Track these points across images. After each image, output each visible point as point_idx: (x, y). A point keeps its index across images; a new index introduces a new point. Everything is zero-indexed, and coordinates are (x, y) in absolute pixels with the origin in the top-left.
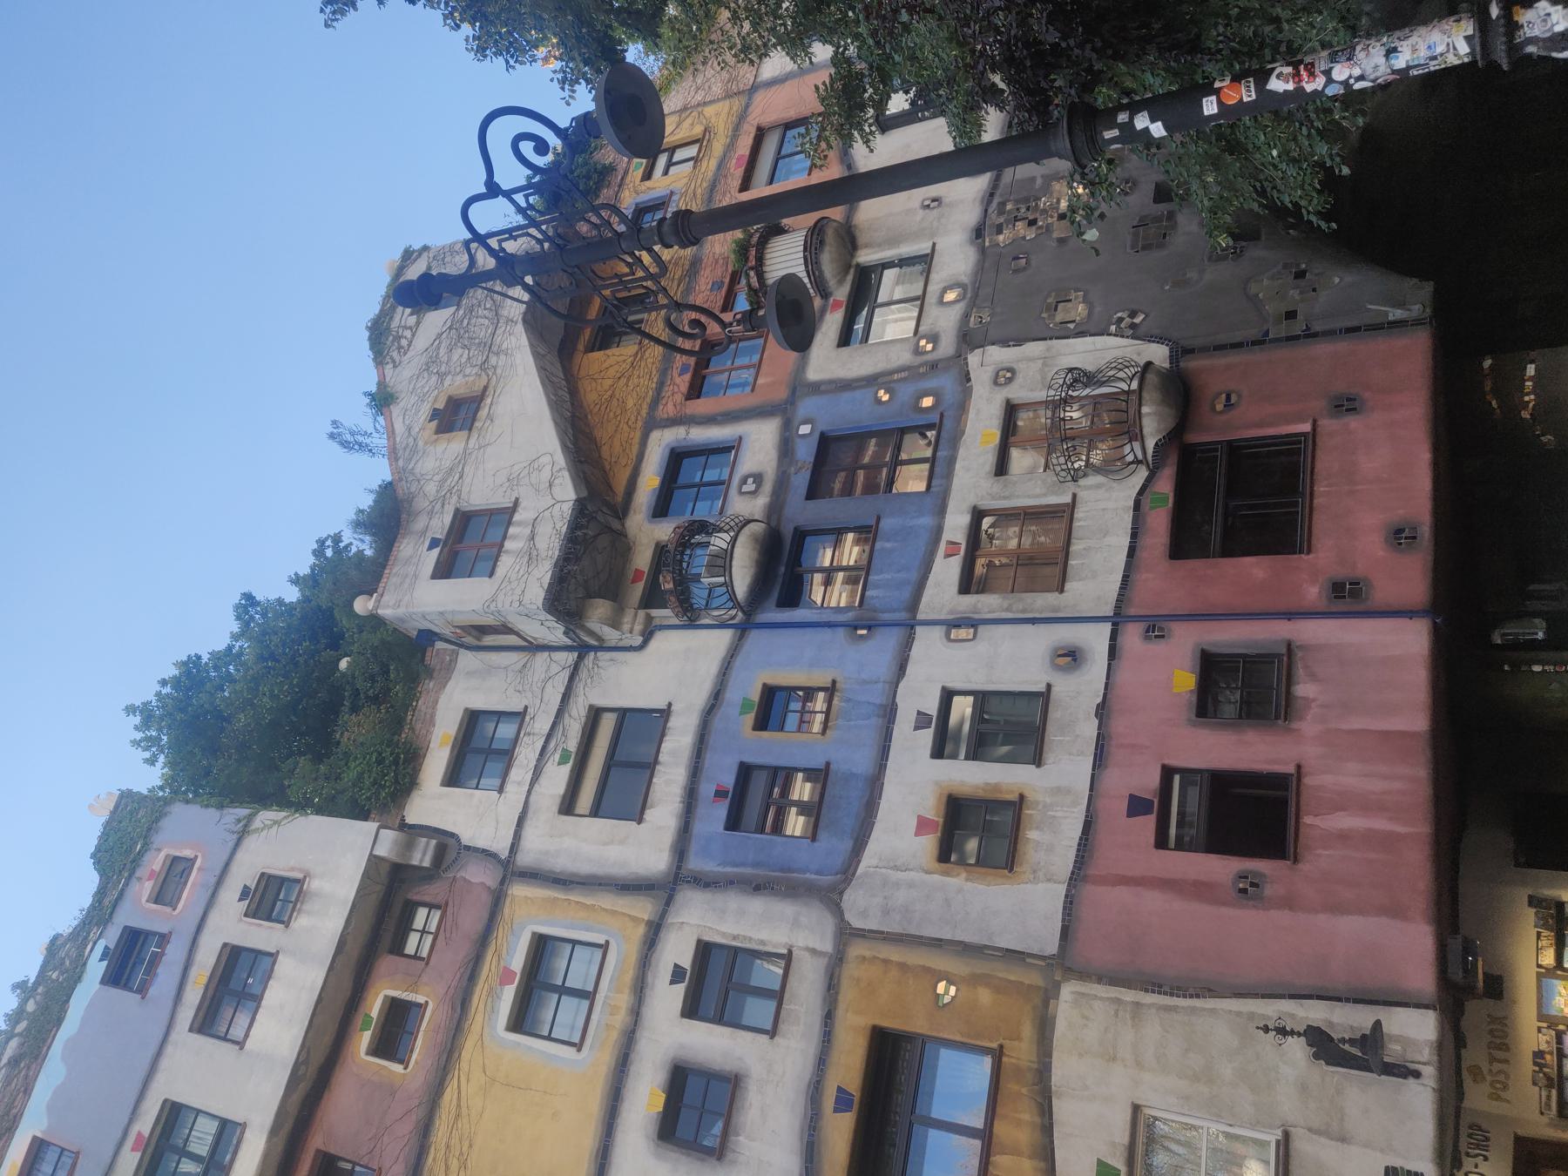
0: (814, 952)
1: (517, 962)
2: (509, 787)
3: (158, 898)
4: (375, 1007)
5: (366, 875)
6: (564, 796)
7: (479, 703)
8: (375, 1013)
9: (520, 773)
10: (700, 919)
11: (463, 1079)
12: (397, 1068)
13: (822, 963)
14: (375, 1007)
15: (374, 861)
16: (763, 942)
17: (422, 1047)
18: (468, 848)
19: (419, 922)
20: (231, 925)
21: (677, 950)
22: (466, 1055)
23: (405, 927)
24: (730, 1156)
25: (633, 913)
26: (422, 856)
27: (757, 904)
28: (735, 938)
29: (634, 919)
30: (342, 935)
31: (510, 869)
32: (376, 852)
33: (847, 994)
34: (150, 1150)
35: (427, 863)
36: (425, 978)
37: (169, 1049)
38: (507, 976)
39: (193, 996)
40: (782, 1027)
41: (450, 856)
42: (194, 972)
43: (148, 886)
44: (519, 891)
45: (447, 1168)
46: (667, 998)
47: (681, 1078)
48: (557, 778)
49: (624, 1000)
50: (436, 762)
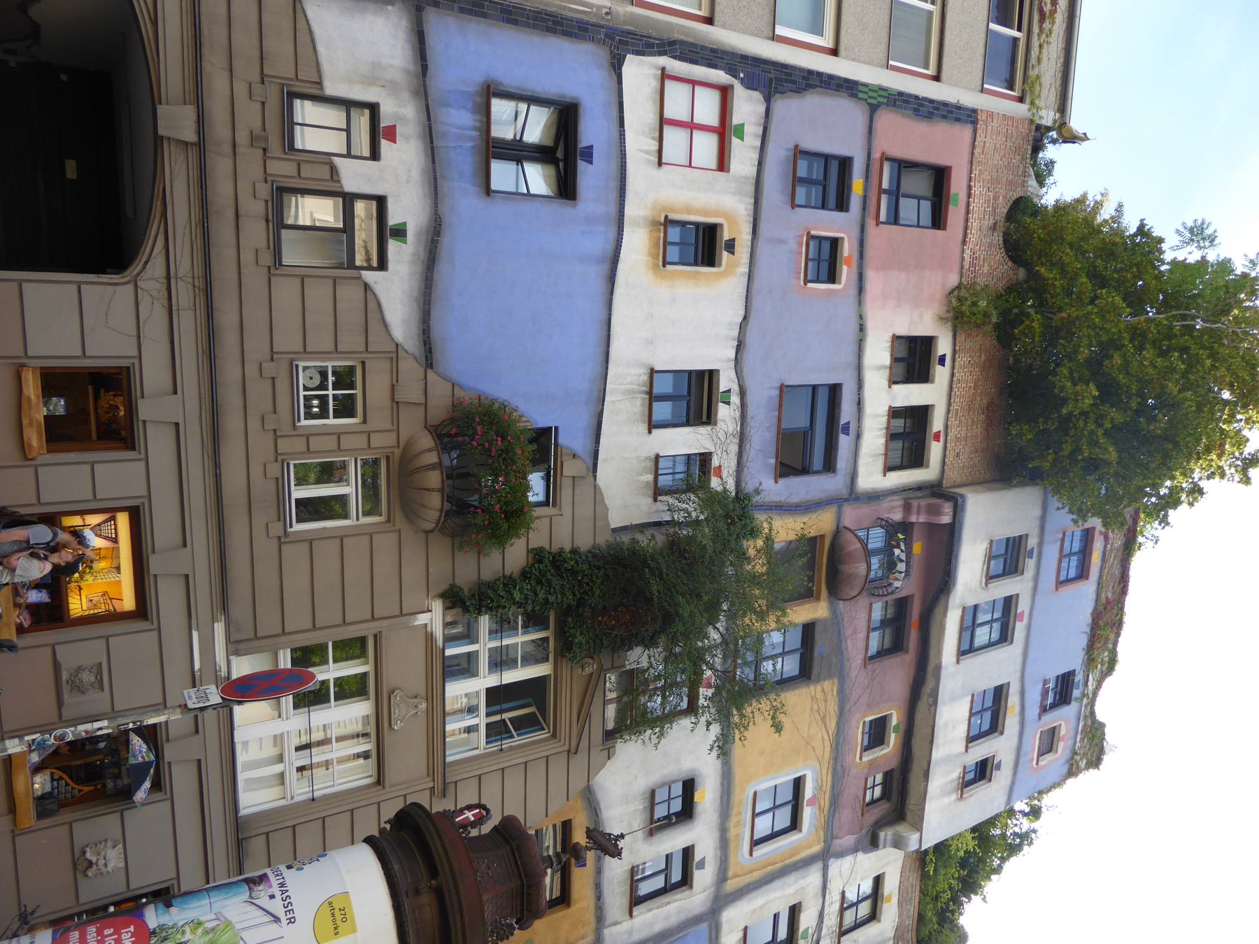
0: (616, 924)
1: (808, 813)
2: (837, 898)
3: (1053, 731)
4: (893, 739)
5: (921, 818)
6: (800, 912)
7: (872, 930)
8: (893, 736)
9: (833, 908)
10: (694, 900)
11: (826, 737)
12: (868, 719)
13: (609, 920)
14: (893, 739)
15: (918, 826)
16: (650, 910)
17: (859, 735)
18: (855, 850)
19: (878, 792)
20: (1001, 747)
21: (703, 878)
22: (828, 749)
23: (886, 783)
24: (648, 795)
25: (738, 879)
26: (886, 835)
27: (658, 928)
28: (669, 903)
29: (736, 876)
30: (927, 781)
31: (824, 857)
32: (917, 835)
33: (590, 916)
34: (1012, 615)
35: (882, 835)
36: (866, 771)
37: (1019, 668)
38: (811, 803)
39: (1013, 700)
40: (628, 875)
41: (867, 841)
42: (1017, 710)
43: (1063, 731)
44: (817, 848)
45: (823, 691)
46: (706, 849)
47: (687, 812)
48: (807, 920)
49: (732, 833)
50: (891, 886)
